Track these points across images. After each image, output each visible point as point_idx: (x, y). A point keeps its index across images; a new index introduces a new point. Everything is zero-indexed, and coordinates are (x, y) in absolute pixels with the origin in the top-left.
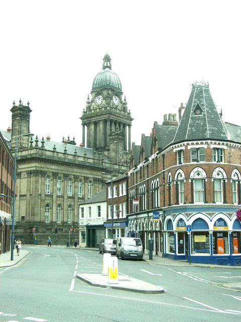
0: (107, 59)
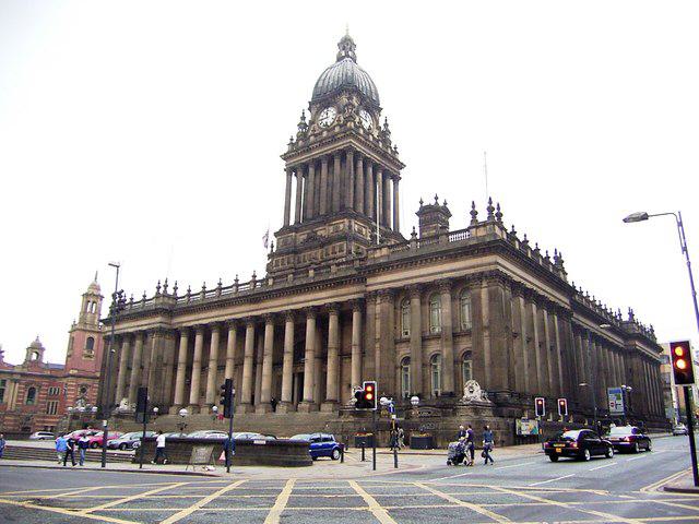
0: (347, 47)
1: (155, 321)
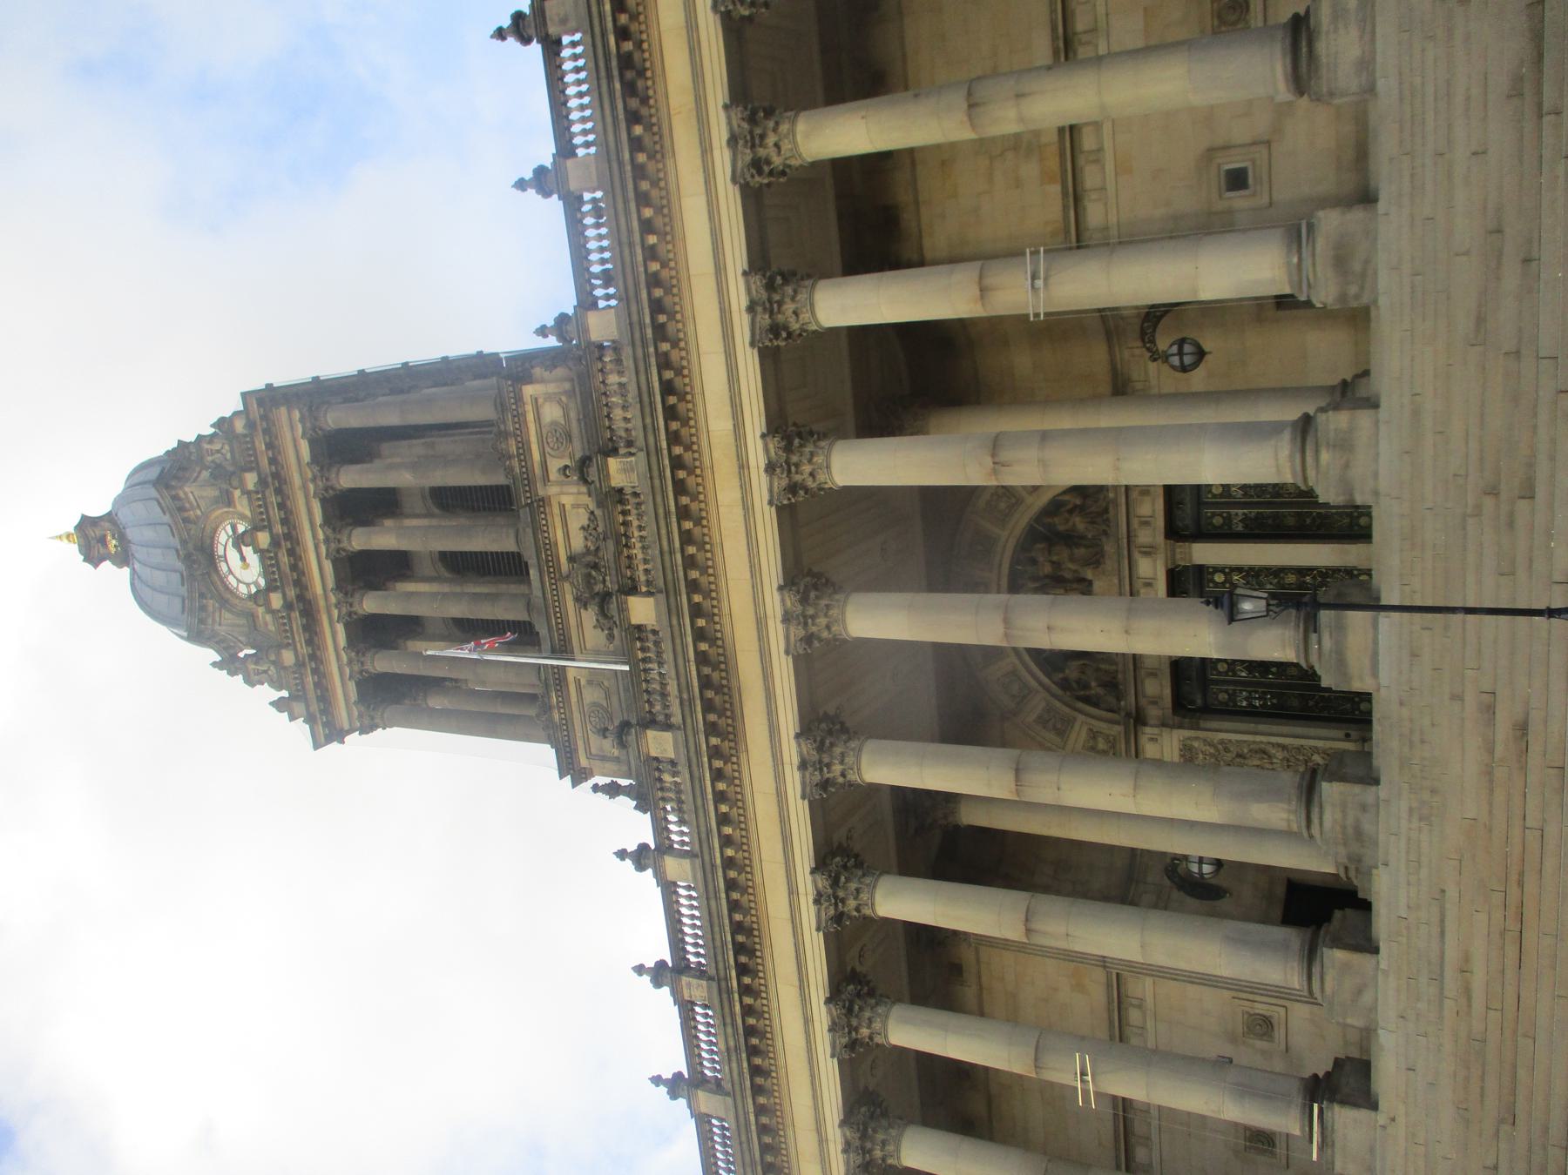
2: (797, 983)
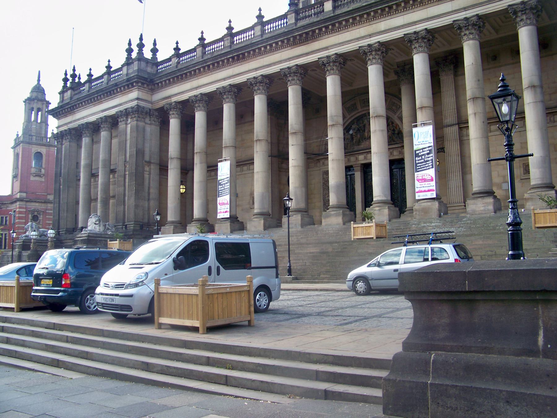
1: (129, 99)
2: (234, 74)
